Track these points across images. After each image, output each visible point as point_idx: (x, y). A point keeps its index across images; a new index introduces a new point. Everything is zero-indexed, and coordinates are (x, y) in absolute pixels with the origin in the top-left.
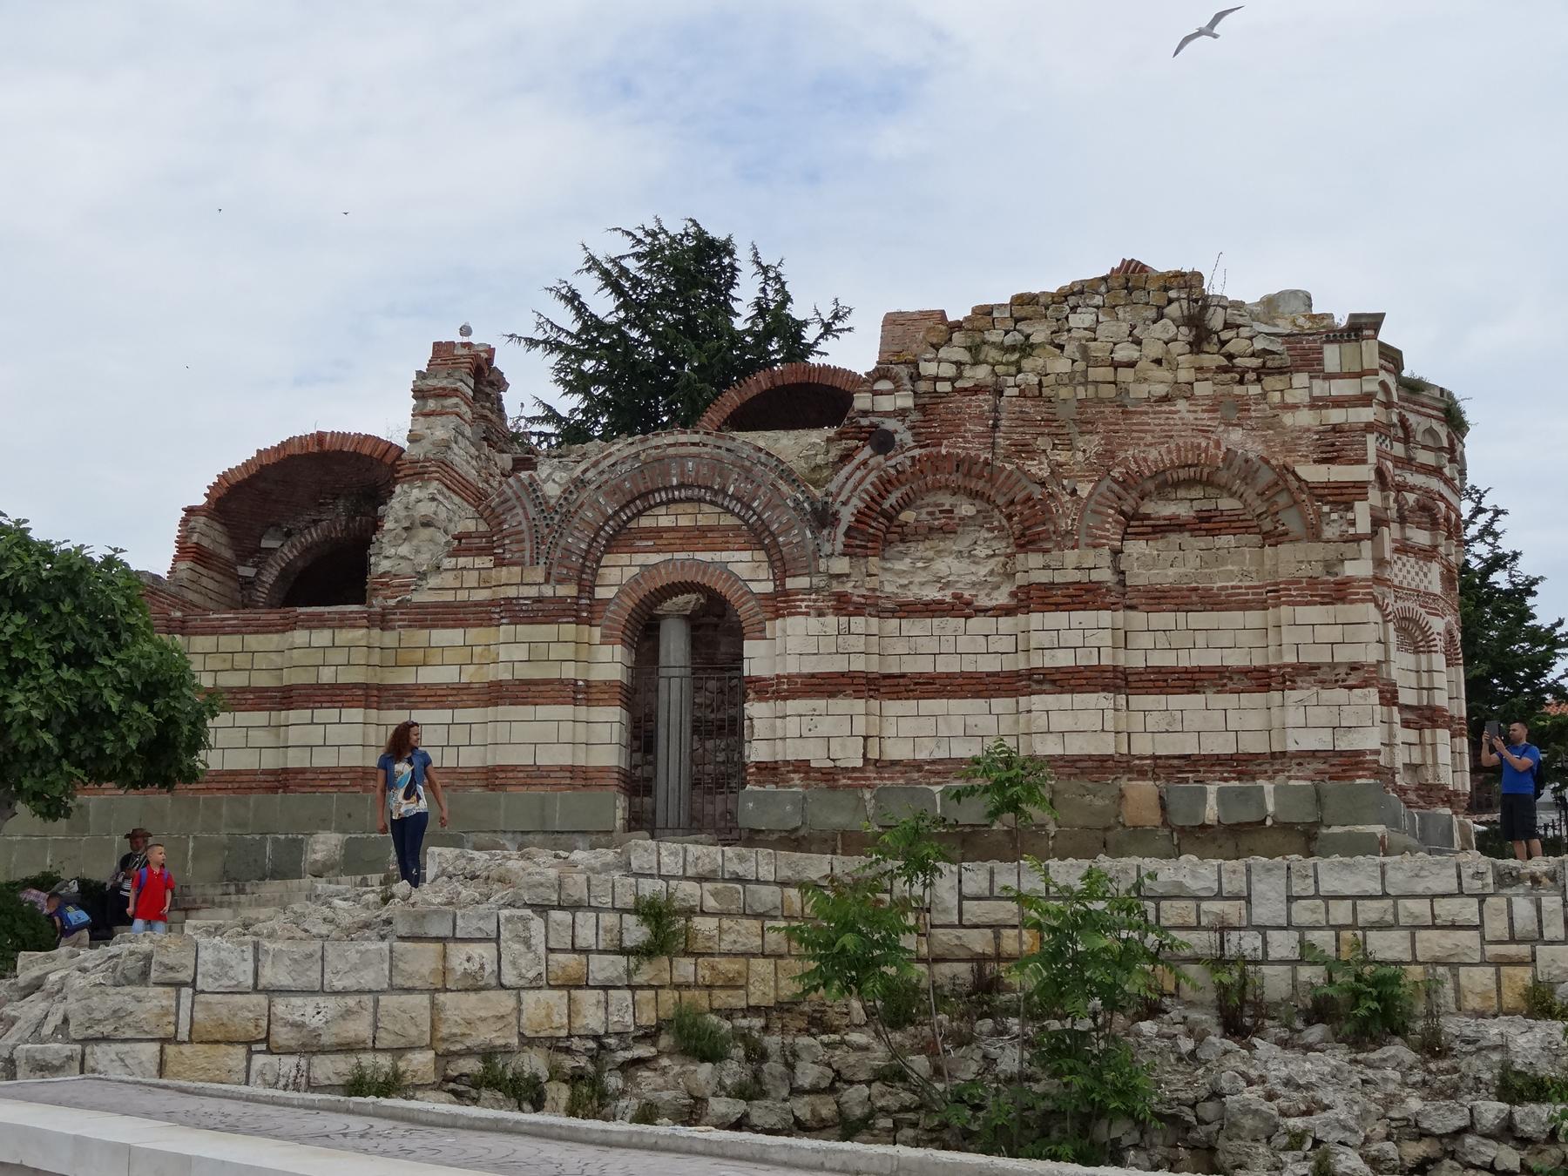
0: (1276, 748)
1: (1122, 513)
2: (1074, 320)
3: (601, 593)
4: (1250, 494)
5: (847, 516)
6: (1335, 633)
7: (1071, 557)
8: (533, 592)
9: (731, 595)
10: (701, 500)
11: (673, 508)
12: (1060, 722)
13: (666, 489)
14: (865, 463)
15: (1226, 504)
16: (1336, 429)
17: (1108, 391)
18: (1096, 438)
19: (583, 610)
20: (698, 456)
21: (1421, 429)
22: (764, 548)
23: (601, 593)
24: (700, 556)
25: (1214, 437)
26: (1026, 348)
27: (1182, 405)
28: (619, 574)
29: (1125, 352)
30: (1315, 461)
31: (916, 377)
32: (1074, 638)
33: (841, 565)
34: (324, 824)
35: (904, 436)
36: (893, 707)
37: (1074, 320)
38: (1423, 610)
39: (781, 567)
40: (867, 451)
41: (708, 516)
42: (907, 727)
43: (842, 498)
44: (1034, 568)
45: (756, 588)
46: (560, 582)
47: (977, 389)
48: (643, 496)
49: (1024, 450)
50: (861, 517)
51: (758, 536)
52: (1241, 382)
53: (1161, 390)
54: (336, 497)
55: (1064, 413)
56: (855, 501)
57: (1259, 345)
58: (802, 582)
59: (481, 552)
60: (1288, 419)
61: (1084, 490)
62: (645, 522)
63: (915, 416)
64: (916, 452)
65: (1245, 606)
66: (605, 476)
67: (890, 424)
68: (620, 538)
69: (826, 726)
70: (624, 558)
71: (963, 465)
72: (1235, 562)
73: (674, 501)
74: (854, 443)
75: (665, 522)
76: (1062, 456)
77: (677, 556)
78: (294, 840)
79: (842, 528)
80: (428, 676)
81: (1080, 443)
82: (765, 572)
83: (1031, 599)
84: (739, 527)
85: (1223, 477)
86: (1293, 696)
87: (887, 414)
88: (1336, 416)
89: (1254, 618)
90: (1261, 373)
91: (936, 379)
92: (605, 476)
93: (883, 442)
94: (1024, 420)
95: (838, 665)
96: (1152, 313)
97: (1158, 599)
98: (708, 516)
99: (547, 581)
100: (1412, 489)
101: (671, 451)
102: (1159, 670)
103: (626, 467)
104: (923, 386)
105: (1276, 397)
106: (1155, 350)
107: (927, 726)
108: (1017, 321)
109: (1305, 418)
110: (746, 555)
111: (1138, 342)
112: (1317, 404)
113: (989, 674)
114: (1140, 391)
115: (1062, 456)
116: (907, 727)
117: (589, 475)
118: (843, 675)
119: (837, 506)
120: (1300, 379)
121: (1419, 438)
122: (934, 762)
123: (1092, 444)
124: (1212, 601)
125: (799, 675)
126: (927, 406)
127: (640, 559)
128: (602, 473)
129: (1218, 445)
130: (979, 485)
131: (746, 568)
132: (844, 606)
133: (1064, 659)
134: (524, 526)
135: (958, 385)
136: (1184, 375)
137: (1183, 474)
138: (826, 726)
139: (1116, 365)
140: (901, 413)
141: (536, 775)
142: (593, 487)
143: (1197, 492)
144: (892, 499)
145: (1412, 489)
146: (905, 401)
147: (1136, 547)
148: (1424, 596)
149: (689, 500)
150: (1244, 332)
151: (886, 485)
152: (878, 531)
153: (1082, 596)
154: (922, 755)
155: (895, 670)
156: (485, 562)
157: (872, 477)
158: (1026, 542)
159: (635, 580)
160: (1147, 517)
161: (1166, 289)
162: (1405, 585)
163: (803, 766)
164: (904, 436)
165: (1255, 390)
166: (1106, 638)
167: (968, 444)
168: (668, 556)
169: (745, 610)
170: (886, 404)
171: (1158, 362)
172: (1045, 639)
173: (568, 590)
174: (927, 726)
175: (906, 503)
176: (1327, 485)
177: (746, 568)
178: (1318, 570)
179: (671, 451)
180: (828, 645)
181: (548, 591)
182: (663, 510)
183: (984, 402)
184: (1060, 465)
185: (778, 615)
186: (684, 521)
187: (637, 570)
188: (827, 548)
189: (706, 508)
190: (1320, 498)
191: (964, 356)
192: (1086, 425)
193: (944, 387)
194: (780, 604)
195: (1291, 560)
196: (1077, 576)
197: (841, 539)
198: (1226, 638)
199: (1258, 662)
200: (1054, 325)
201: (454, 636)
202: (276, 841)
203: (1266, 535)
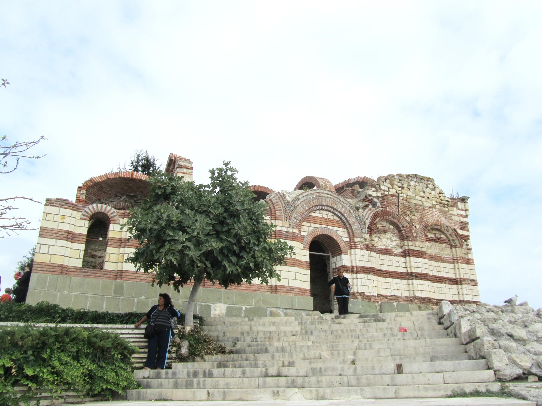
0: (462, 299)
2: (412, 183)
3: (303, 234)
4: (448, 234)
6: (468, 271)
7: (417, 243)
8: (286, 229)
9: (338, 241)
10: (330, 211)
11: (321, 212)
12: (420, 288)
13: (321, 205)
14: (370, 209)
15: (443, 236)
16: (462, 222)
17: (420, 203)
18: (419, 214)
20: (330, 198)
22: (347, 228)
24: (329, 227)
26: (403, 188)
27: (434, 210)
29: (422, 194)
34: (219, 300)
35: (379, 204)
37: (412, 183)
40: (370, 206)
41: (331, 216)
43: (366, 217)
45: (345, 239)
46: (293, 228)
47: (393, 196)
48: (315, 206)
49: (404, 213)
51: (344, 223)
52: (444, 207)
53: (430, 205)
54: (123, 195)
55: (412, 206)
56: (369, 219)
57: (446, 199)
60: (453, 217)
61: (418, 227)
62: (314, 214)
63: (381, 199)
64: (382, 209)
65: (449, 262)
66: (304, 198)
67: (375, 200)
68: (306, 218)
69: (368, 283)
70: (308, 224)
72: (445, 251)
73: (322, 209)
74: (368, 203)
75: (319, 215)
76: (413, 217)
77: (323, 226)
78: (208, 305)
79: (367, 226)
81: (416, 214)
82: (346, 235)
84: (338, 221)
85: (443, 229)
86: (464, 286)
87: (374, 197)
88: (462, 219)
89: (452, 266)
90: (448, 205)
91: (384, 191)
92: (304, 198)
93: (374, 205)
96: (426, 186)
99: (290, 227)
101: (322, 195)
102: (435, 277)
103: (310, 197)
105: (451, 212)
106: (428, 195)
107: (388, 286)
108: (400, 180)
109: (456, 218)
110: (341, 229)
111: (424, 192)
112: (459, 215)
113: (401, 273)
114: (427, 204)
115: (413, 217)
117: (300, 197)
118: (370, 268)
119: (365, 219)
120: (455, 209)
122: (390, 296)
123: (418, 215)
124: (443, 260)
125: (360, 267)
127: (313, 225)
128: (304, 197)
130: (395, 221)
134: (282, 208)
135: (390, 193)
136: (434, 203)
137: (436, 227)
139: (421, 197)
140: (378, 197)
142: (301, 200)
143: (436, 232)
146: (380, 195)
149: (326, 210)
150: (443, 195)
153: (420, 254)
154: (388, 294)
155: (379, 269)
157: (372, 213)
159: (313, 232)
161: (428, 181)
163: (362, 294)
164: (379, 204)
165: (447, 209)
167: (392, 209)
168: (321, 226)
169: (342, 245)
170: (374, 194)
171: (428, 198)
174: (388, 286)
176: (463, 235)
178: (463, 255)
179: (322, 195)
180: (366, 259)
181: (290, 230)
182: (318, 212)
183: (395, 199)
184: (412, 219)
185: (351, 248)
186: (325, 216)
187: (312, 228)
188: (364, 231)
189: (330, 213)
190: (462, 238)
191: (390, 186)
192: (417, 210)
193: (386, 193)
194: (352, 245)
195: (459, 252)
196: (418, 249)
197: (367, 229)
198: (447, 270)
199: (454, 277)
202: (201, 305)
203: (451, 245)
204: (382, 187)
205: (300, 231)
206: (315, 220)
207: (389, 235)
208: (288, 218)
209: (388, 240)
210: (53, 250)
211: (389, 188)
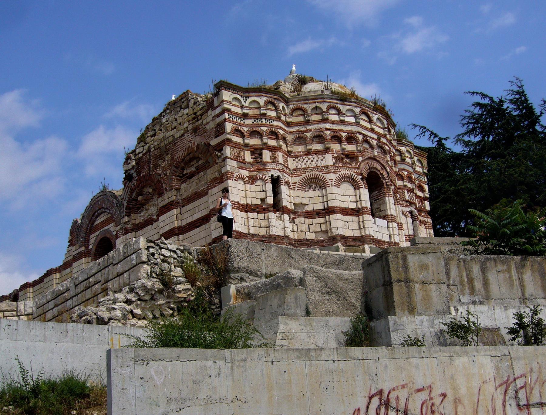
1: (178, 176)
8: (77, 252)
17: (171, 139)
21: (311, 108)
23: (91, 247)
25: (193, 142)
29: (175, 124)
30: (215, 138)
33: (126, 219)
38: (321, 173)
60: (208, 127)
75: (99, 221)
91: (139, 153)
97: (189, 200)
100: (310, 131)
104: (137, 157)
105: (204, 122)
121: (309, 112)
129: (194, 144)
144: (134, 194)
145: (310, 131)
147: (183, 186)
148: (326, 169)
160: (187, 174)
162: (310, 166)
173: (83, 248)
193: (141, 155)
200: (160, 124)
211: (143, 146)
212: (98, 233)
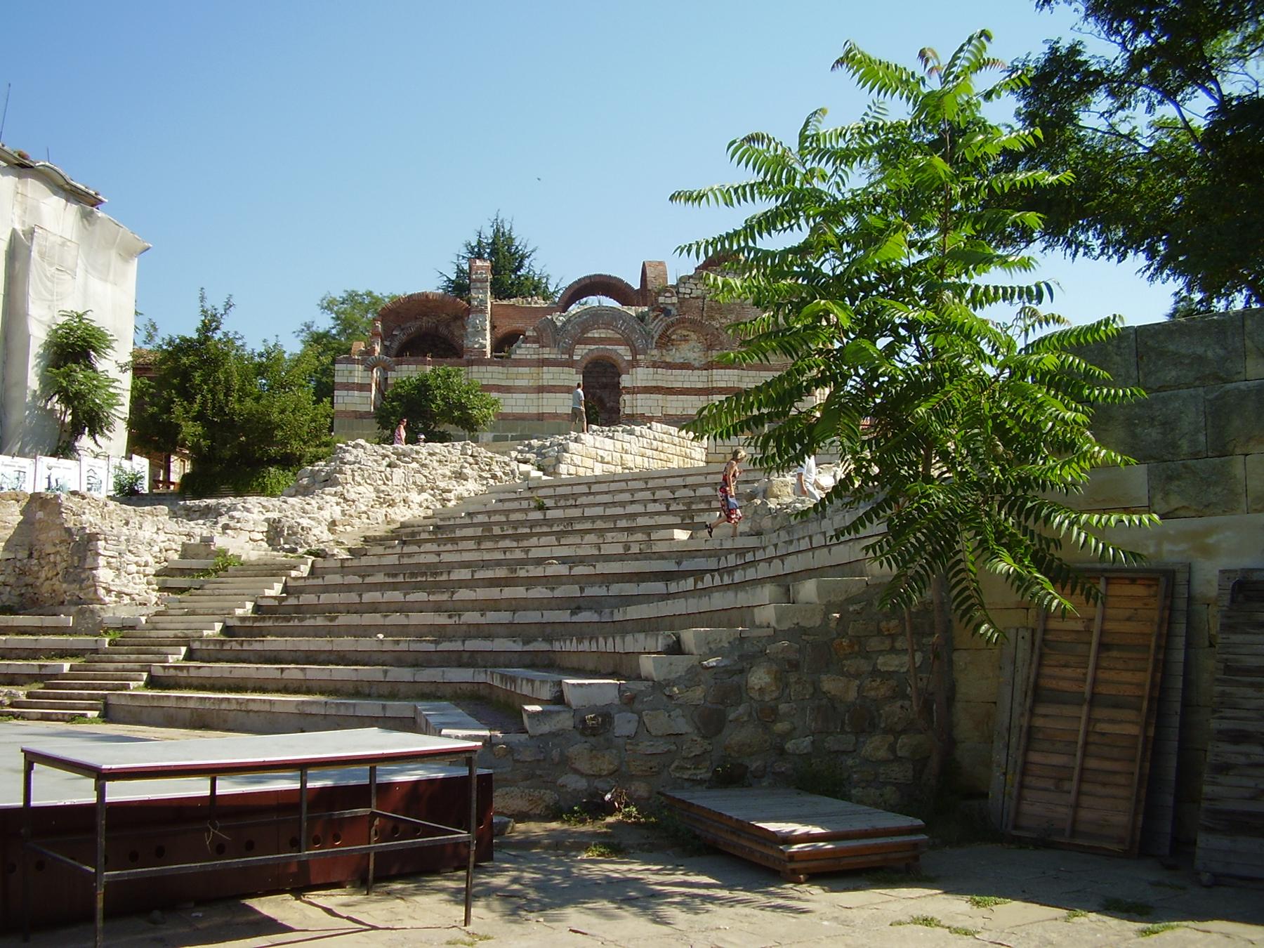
3: (575, 358)
5: (656, 337)
19: (570, 364)
28: (580, 352)
31: (678, 293)
32: (726, 378)
36: (669, 397)
39: (635, 352)
41: (610, 334)
42: (675, 404)
44: (715, 355)
47: (697, 298)
50: (661, 337)
51: (627, 342)
58: (642, 357)
59: (534, 342)
67: (670, 307)
69: (650, 403)
71: (692, 322)
76: (723, 321)
80: (518, 383)
82: (629, 353)
83: (709, 366)
93: (667, 312)
94: (711, 308)
95: (654, 384)
98: (610, 334)
115: (723, 321)
116: (675, 404)
123: (733, 317)
126: (682, 301)
131: (624, 352)
132: (655, 365)
133: (723, 385)
138: (650, 403)
141: (555, 416)
146: (675, 300)
151: (668, 327)
152: (665, 341)
156: (535, 346)
158: (710, 347)
164: (674, 311)
166: (736, 378)
169: (624, 365)
170: (669, 301)
172: (718, 378)
174: (681, 404)
175: (673, 332)
177: (624, 352)
180: (650, 377)
192: (731, 311)
194: (634, 364)
201: (526, 370)
204: (682, 290)
205: (571, 356)
206: (593, 341)
207: (692, 343)
208: (556, 343)
209: (690, 350)
210: (347, 400)
212: (593, 347)
